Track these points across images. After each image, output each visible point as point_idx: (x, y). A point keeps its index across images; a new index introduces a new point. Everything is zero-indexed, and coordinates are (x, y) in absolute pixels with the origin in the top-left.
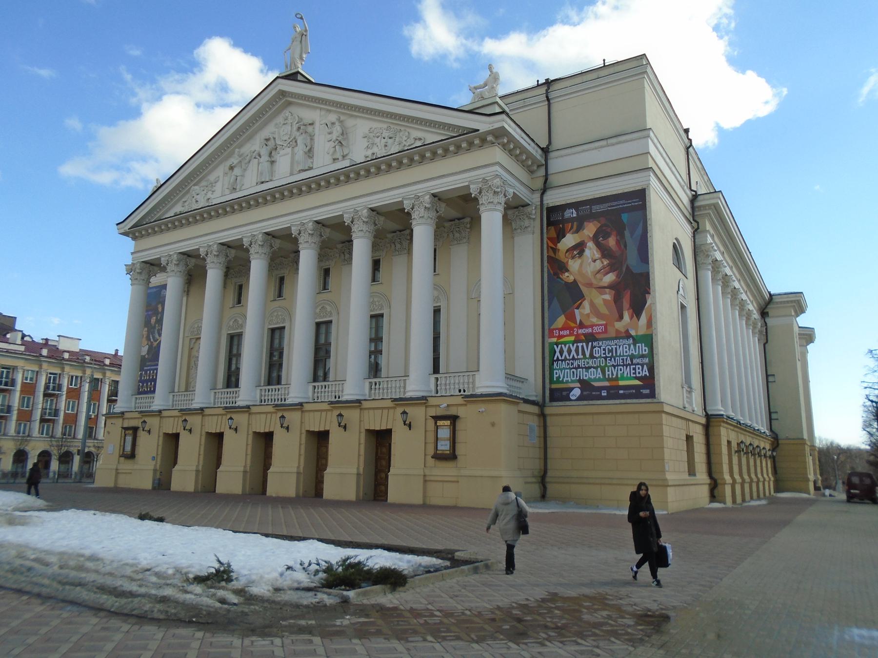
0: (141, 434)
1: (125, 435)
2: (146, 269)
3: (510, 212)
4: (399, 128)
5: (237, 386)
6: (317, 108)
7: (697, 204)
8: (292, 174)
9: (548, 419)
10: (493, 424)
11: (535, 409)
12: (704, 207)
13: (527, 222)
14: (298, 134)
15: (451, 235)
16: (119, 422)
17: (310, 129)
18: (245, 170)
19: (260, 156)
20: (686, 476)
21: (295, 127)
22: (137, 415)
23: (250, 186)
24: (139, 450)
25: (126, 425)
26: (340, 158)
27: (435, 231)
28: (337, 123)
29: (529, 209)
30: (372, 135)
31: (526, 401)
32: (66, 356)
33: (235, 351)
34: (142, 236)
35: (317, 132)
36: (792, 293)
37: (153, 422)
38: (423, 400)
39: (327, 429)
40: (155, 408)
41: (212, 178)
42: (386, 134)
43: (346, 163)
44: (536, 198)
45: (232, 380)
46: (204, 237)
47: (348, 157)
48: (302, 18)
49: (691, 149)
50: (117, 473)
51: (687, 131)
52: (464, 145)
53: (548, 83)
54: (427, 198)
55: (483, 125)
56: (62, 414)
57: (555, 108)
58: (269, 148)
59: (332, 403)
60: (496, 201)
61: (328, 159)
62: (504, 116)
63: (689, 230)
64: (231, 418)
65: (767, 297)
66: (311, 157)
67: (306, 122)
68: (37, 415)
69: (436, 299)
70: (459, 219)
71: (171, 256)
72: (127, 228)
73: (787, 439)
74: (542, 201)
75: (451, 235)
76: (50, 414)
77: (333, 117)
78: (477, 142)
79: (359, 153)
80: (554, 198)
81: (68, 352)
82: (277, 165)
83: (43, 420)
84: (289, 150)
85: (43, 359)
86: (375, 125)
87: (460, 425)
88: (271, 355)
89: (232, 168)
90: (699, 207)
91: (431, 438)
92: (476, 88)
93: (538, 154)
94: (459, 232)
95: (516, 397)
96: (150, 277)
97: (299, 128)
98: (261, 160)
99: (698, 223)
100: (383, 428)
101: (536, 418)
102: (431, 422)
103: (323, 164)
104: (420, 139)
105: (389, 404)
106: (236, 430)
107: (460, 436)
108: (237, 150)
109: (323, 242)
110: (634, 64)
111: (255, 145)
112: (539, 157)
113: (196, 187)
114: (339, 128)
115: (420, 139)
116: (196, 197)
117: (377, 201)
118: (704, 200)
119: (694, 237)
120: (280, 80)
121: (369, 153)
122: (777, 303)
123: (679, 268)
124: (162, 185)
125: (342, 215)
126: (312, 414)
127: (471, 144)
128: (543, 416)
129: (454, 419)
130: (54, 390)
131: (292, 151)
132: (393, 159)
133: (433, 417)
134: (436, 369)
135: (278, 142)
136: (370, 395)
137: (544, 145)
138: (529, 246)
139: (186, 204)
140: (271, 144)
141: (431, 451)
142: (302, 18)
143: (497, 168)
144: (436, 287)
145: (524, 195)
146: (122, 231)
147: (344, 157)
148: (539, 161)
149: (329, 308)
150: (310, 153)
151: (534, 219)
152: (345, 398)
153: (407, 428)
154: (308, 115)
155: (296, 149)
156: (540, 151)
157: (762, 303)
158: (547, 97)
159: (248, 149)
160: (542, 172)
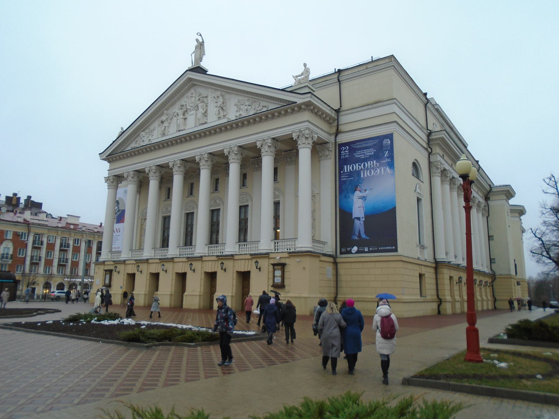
0: (115, 274)
1: (106, 274)
2: (116, 180)
3: (318, 147)
4: (254, 100)
5: (168, 246)
6: (208, 88)
7: (431, 138)
8: (195, 126)
9: (339, 266)
10: (304, 269)
11: (331, 260)
12: (436, 139)
13: (327, 153)
14: (199, 102)
15: (286, 159)
16: (102, 268)
17: (205, 100)
18: (170, 123)
19: (178, 115)
20: (419, 297)
21: (197, 98)
22: (112, 263)
23: (172, 133)
24: (114, 283)
25: (106, 269)
26: (222, 117)
27: (275, 159)
28: (221, 97)
29: (328, 145)
30: (239, 104)
31: (325, 255)
32: (72, 227)
33: (166, 226)
34: (114, 161)
35: (209, 101)
36: (504, 186)
37: (120, 267)
38: (266, 255)
39: (215, 271)
40: (122, 259)
41: (152, 127)
42: (247, 103)
43: (225, 120)
44: (333, 137)
45: (165, 243)
46: (147, 163)
47: (227, 116)
48: (200, 35)
49: (429, 105)
51: (425, 94)
52: (289, 110)
53: (340, 71)
54: (269, 141)
55: (299, 100)
56: (70, 261)
57: (342, 85)
58: (182, 111)
59: (217, 256)
60: (306, 142)
61: (215, 118)
62: (309, 95)
63: (426, 154)
64: (163, 265)
65: (488, 188)
66: (206, 116)
67: (203, 95)
68: (55, 263)
69: (275, 196)
70: (290, 150)
71: (129, 172)
72: (104, 157)
73: (501, 275)
74: (335, 140)
75: (286, 159)
76: (63, 261)
77: (219, 93)
78: (296, 109)
79: (232, 115)
80: (343, 138)
81: (73, 224)
82: (188, 120)
83: (59, 265)
84: (194, 112)
85: (59, 229)
86: (241, 98)
87: (287, 269)
88: (187, 228)
89: (162, 122)
90: (433, 139)
91: (271, 276)
92: (297, 77)
93: (333, 114)
94: (290, 158)
95: (318, 253)
96: (118, 184)
97: (199, 100)
98: (179, 118)
99: (431, 149)
100: (246, 270)
101: (331, 265)
102: (271, 267)
103: (213, 121)
104: (266, 107)
105: (249, 257)
106: (166, 271)
107: (287, 275)
108: (165, 111)
109: (213, 165)
110: (387, 61)
111: (176, 109)
112: (333, 115)
113: (143, 133)
114: (222, 100)
115: (266, 107)
117: (243, 142)
118: (435, 135)
119: (429, 157)
120: (188, 72)
121: (238, 114)
122: (495, 192)
123: (418, 177)
124: (124, 131)
125: (223, 150)
126: (207, 262)
128: (335, 263)
129: (283, 266)
130: (65, 247)
131: (196, 113)
132: (251, 118)
133: (272, 264)
134: (276, 237)
135: (188, 107)
136: (239, 252)
137: (337, 107)
138: (328, 166)
140: (184, 109)
141: (271, 283)
142: (200, 35)
143: (307, 123)
144: (275, 189)
145: (325, 136)
146: (102, 158)
147: (224, 116)
148: (333, 118)
149: (218, 202)
150: (205, 114)
151: (331, 151)
152: (225, 254)
153: (258, 270)
154: (204, 92)
155: (198, 112)
156: (334, 112)
157: (486, 192)
158: (338, 80)
160: (335, 124)
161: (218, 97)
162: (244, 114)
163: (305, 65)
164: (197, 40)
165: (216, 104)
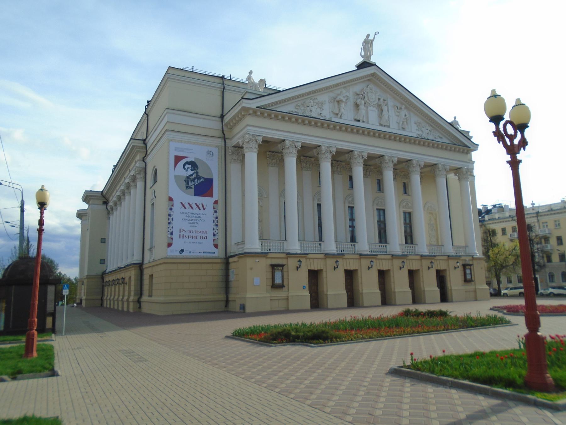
22: (283, 255)
42: (429, 129)
48: (375, 34)
50: (271, 300)
121: (420, 133)
139: (298, 107)
142: (375, 34)
161: (401, 108)
162: (424, 136)
163: (455, 118)
164: (368, 36)
165: (398, 114)
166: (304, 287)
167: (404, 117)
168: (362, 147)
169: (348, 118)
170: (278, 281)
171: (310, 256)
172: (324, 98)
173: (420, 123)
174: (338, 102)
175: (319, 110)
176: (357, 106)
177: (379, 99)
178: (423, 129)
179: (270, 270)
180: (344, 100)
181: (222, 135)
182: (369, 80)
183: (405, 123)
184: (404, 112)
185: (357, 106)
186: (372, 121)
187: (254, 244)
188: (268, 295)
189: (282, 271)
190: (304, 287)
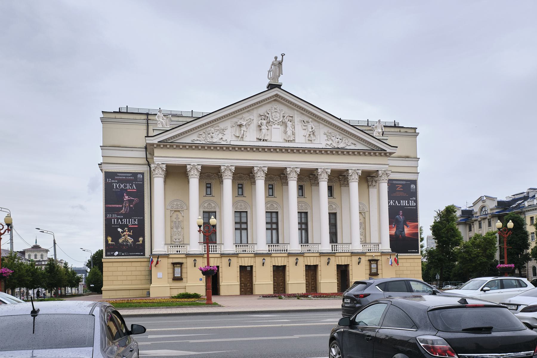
6: (294, 109)
41: (222, 125)
46: (227, 162)
47: (315, 142)
79: (321, 141)
86: (330, 131)
89: (240, 126)
98: (263, 127)
111: (254, 116)
113: (212, 129)
116: (212, 134)
121: (329, 143)
127: (380, 154)
135: (271, 120)
159: (247, 116)
161: (308, 122)
165: (304, 128)
166: (201, 280)
167: (311, 130)
168: (261, 163)
169: (251, 138)
170: (178, 275)
171: (240, 255)
172: (227, 124)
173: (330, 133)
174: (240, 126)
175: (221, 136)
176: (260, 126)
177: (284, 117)
178: (332, 138)
179: (172, 267)
180: (244, 123)
181: (147, 163)
182: (275, 100)
183: (312, 135)
184: (312, 124)
185: (260, 126)
186: (276, 138)
187: (160, 247)
188: (168, 285)
189: (181, 267)
190: (201, 280)
